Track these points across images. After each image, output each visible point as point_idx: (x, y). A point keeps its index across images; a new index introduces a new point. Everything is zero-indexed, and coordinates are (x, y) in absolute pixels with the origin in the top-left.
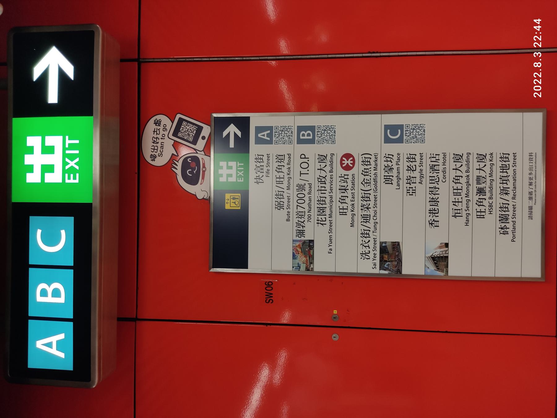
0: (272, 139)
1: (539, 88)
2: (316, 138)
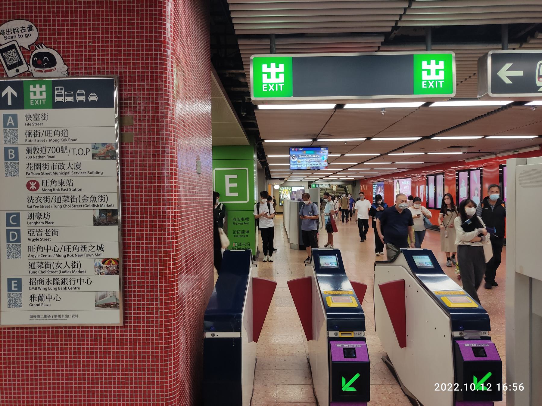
0: (8, 127)
1: (444, 389)
2: (9, 162)
